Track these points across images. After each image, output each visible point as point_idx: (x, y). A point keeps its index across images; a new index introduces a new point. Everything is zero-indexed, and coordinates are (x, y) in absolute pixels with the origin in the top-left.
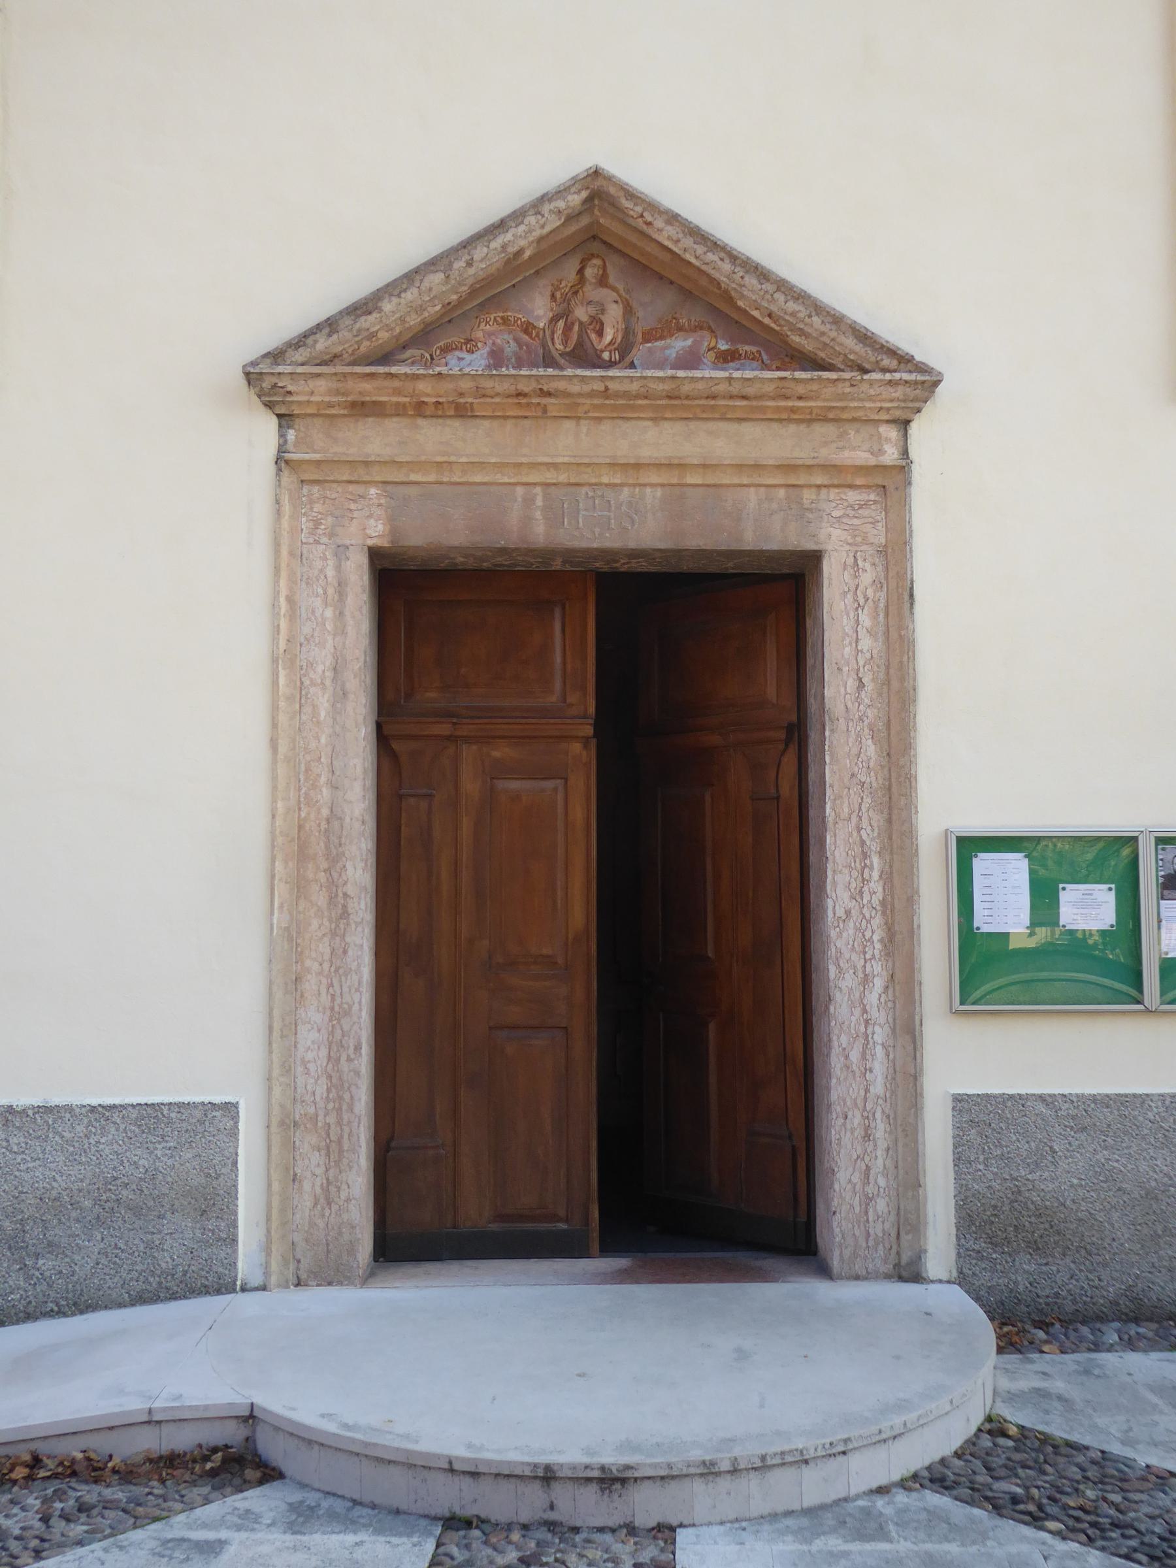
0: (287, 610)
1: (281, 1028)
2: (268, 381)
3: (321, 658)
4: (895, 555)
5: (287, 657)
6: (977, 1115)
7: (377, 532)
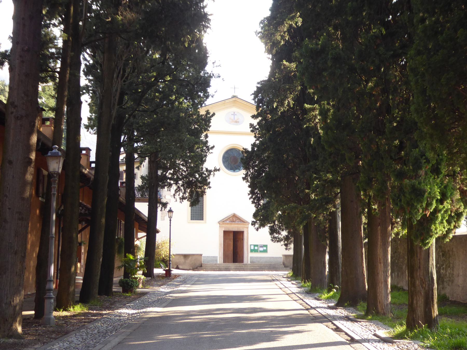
1: (219, 253)
2: (219, 223)
4: (248, 231)
5: (220, 236)
6: (251, 257)
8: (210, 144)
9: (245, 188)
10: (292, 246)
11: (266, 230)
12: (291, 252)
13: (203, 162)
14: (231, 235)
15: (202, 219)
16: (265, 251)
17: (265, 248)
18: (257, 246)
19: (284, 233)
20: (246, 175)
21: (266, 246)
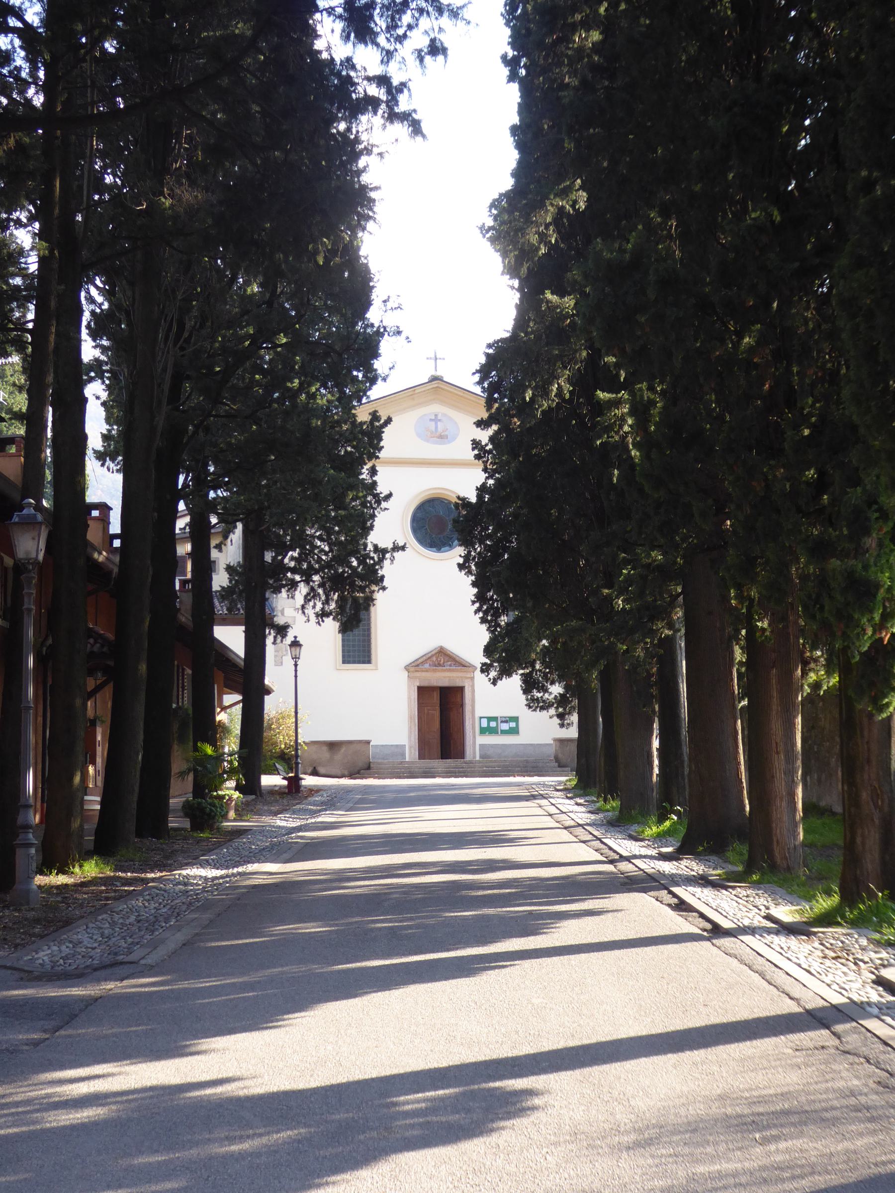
0: (409, 692)
1: (410, 737)
2: (407, 668)
3: (412, 698)
4: (473, 686)
5: (409, 698)
7: (418, 684)
8: (382, 489)
9: (464, 587)
10: (575, 718)
11: (515, 682)
12: (573, 733)
13: (367, 530)
14: (436, 697)
15: (369, 662)
16: (515, 731)
17: (513, 725)
18: (495, 719)
19: (556, 690)
20: (467, 558)
21: (516, 719)
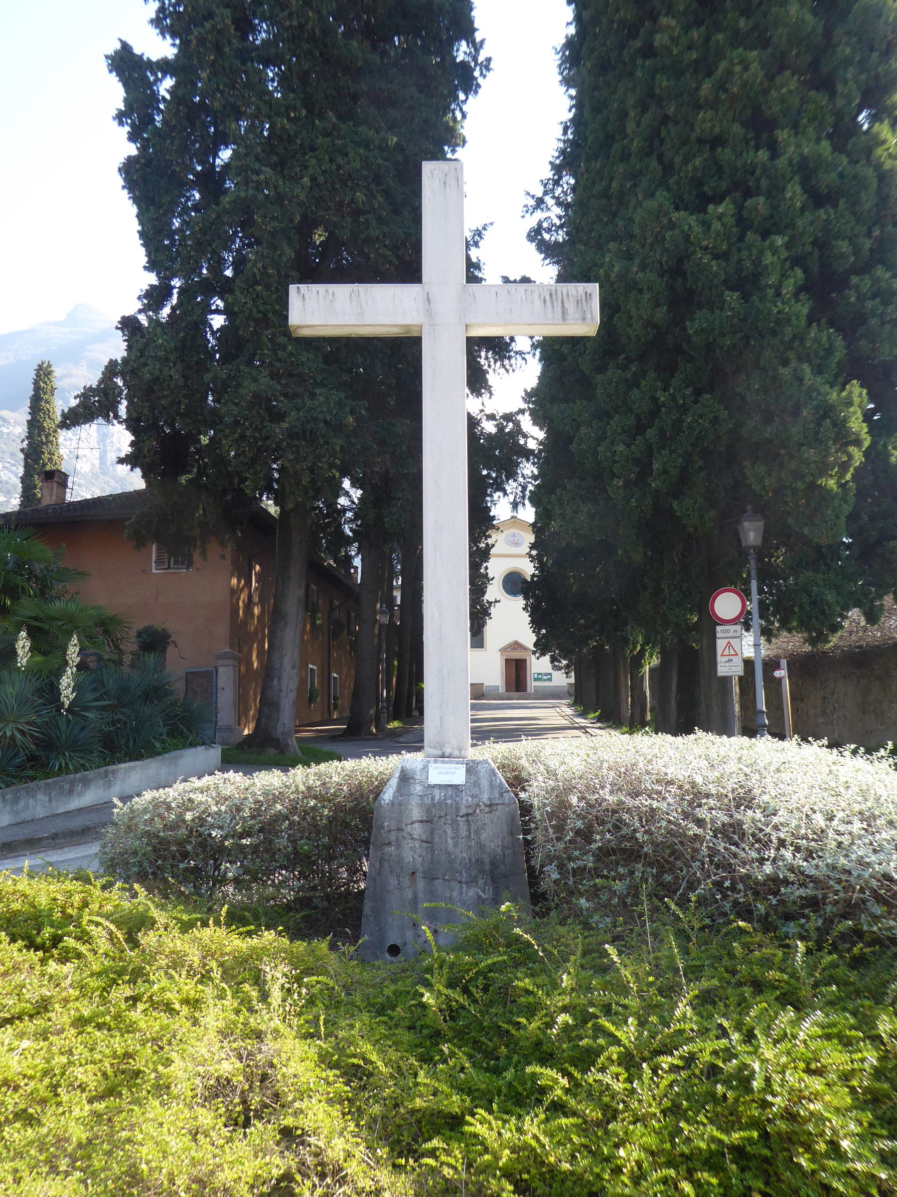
8: (490, 576)
9: (526, 618)
10: (573, 674)
12: (572, 680)
13: (484, 593)
16: (550, 680)
20: (526, 605)
